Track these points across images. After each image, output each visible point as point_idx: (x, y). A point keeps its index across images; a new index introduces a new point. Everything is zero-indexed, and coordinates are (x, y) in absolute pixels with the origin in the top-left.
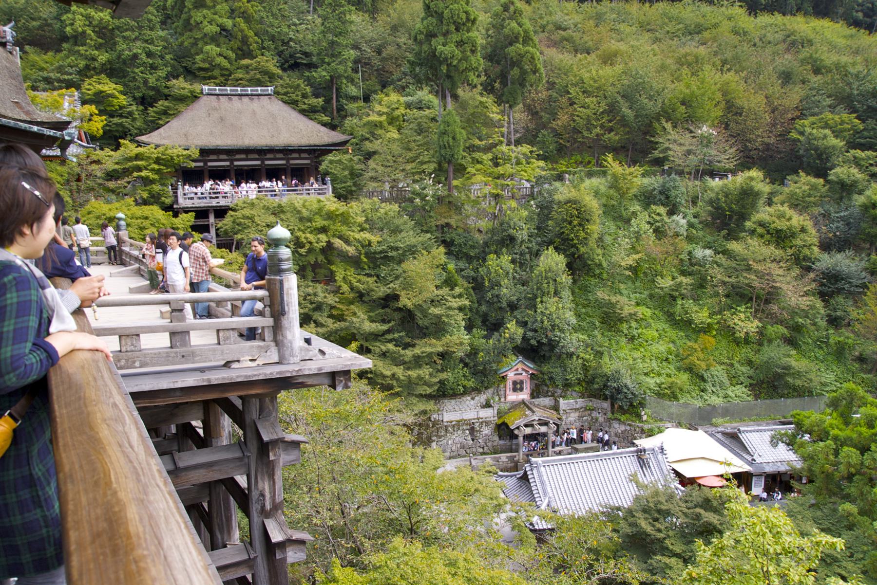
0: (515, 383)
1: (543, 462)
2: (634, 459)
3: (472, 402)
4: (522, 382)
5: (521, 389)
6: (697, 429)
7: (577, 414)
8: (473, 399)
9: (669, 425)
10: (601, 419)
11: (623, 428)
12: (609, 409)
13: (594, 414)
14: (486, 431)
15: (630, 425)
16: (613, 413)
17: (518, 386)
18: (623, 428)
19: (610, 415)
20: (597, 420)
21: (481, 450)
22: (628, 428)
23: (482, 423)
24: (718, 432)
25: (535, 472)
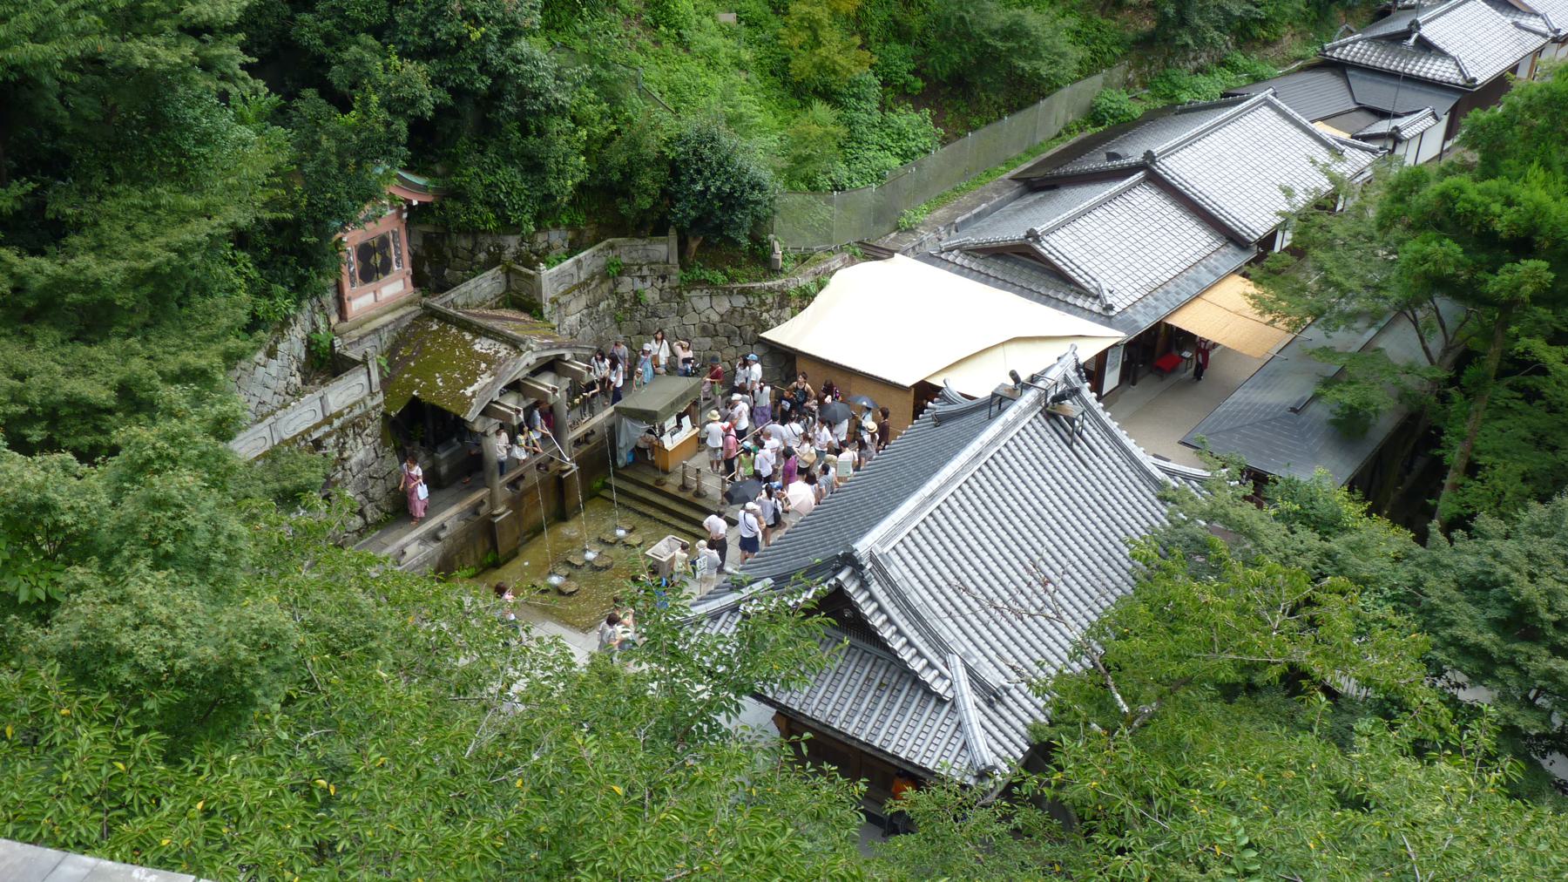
0: (365, 251)
1: (883, 542)
2: (1042, 425)
3: (274, 366)
4: (384, 242)
5: (386, 268)
6: (890, 253)
7: (584, 300)
8: (271, 354)
9: (836, 261)
10: (651, 295)
11: (723, 305)
12: (674, 260)
13: (627, 285)
14: (360, 452)
15: (744, 292)
16: (684, 265)
17: (377, 260)
18: (723, 305)
19: (676, 274)
20: (637, 298)
21: (357, 522)
22: (740, 302)
23: (342, 428)
24: (950, 250)
25: (875, 588)
